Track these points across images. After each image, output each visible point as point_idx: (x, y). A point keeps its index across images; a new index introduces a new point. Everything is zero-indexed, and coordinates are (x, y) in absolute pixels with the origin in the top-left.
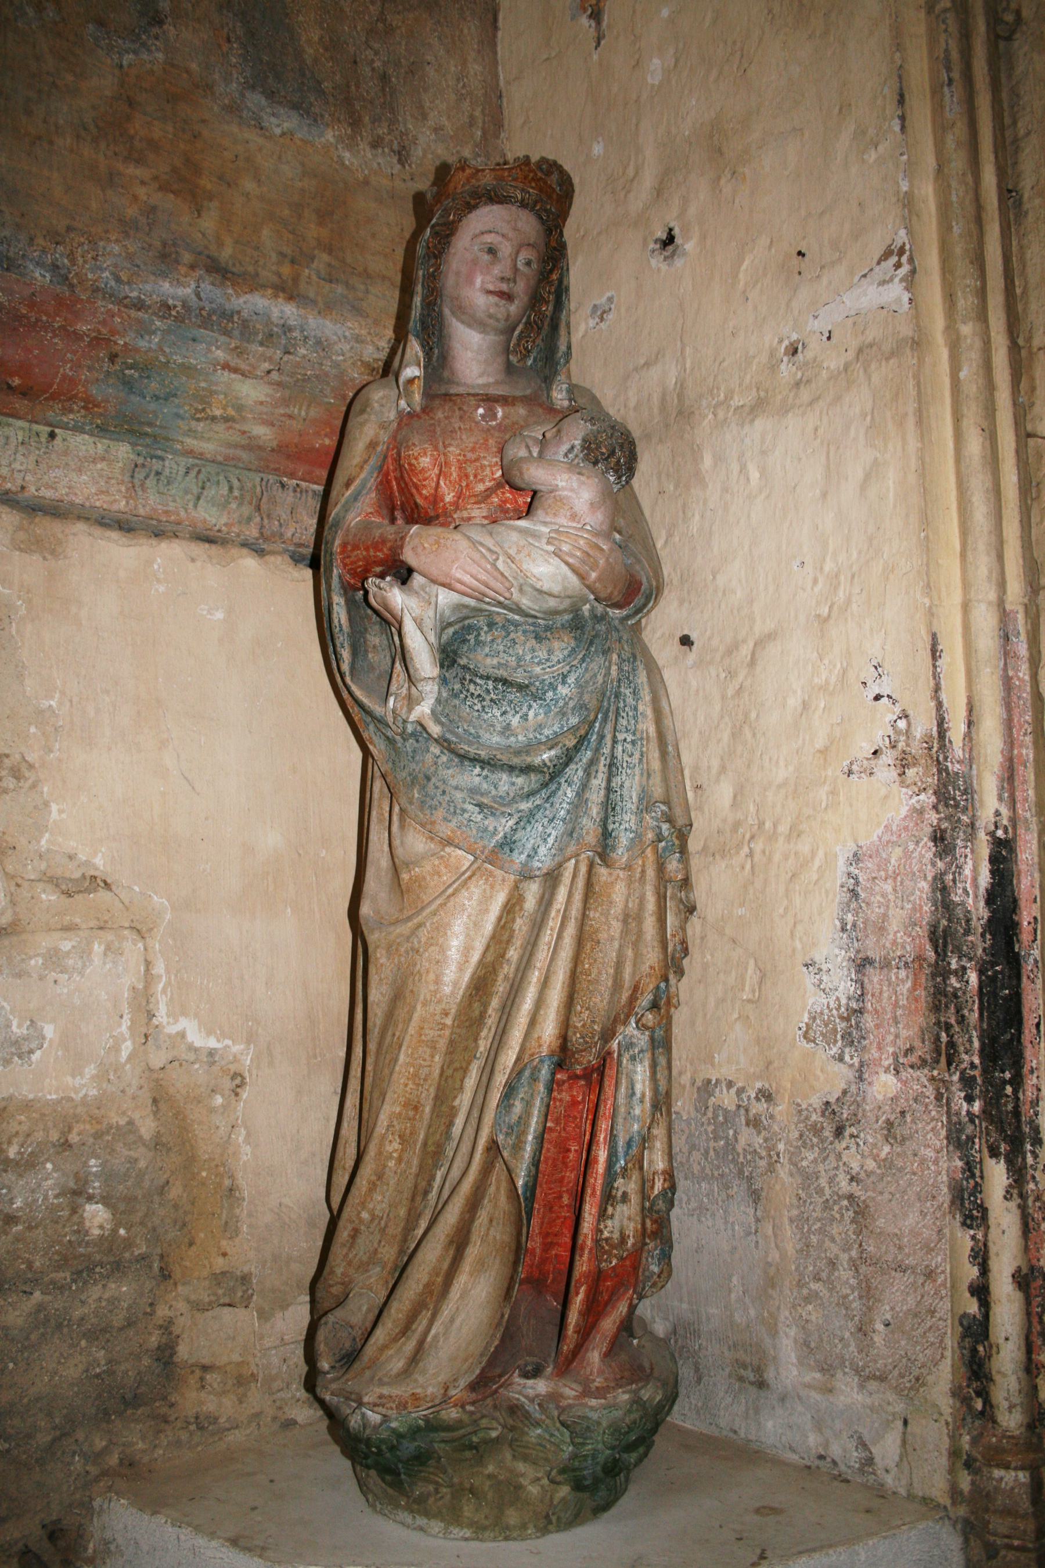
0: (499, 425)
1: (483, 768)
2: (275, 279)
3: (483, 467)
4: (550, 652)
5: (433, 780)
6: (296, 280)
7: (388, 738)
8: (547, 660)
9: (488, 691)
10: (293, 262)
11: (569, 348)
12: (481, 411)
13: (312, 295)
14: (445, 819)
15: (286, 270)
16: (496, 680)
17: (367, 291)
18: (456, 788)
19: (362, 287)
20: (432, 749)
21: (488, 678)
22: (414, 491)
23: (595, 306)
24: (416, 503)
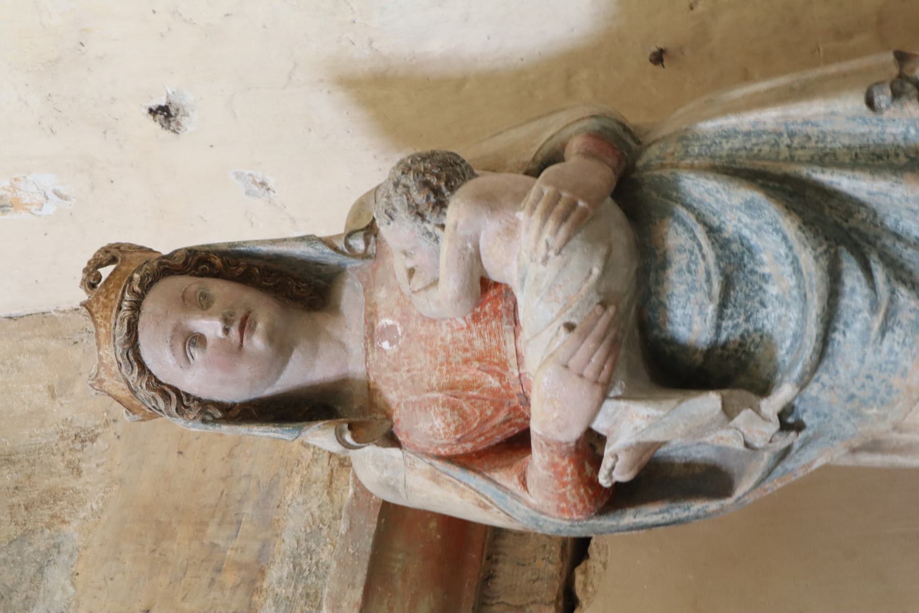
0: (401, 322)
1: (835, 330)
2: (240, 593)
3: (454, 341)
4: (681, 250)
5: (853, 390)
6: (240, 566)
7: (802, 447)
8: (692, 253)
9: (736, 326)
10: (219, 570)
11: (302, 239)
12: (386, 345)
13: (256, 546)
14: (904, 374)
15: (230, 578)
16: (720, 316)
17: (249, 476)
18: (862, 361)
19: (243, 483)
21: (718, 327)
22: (488, 426)
23: (247, 193)
24: (504, 422)
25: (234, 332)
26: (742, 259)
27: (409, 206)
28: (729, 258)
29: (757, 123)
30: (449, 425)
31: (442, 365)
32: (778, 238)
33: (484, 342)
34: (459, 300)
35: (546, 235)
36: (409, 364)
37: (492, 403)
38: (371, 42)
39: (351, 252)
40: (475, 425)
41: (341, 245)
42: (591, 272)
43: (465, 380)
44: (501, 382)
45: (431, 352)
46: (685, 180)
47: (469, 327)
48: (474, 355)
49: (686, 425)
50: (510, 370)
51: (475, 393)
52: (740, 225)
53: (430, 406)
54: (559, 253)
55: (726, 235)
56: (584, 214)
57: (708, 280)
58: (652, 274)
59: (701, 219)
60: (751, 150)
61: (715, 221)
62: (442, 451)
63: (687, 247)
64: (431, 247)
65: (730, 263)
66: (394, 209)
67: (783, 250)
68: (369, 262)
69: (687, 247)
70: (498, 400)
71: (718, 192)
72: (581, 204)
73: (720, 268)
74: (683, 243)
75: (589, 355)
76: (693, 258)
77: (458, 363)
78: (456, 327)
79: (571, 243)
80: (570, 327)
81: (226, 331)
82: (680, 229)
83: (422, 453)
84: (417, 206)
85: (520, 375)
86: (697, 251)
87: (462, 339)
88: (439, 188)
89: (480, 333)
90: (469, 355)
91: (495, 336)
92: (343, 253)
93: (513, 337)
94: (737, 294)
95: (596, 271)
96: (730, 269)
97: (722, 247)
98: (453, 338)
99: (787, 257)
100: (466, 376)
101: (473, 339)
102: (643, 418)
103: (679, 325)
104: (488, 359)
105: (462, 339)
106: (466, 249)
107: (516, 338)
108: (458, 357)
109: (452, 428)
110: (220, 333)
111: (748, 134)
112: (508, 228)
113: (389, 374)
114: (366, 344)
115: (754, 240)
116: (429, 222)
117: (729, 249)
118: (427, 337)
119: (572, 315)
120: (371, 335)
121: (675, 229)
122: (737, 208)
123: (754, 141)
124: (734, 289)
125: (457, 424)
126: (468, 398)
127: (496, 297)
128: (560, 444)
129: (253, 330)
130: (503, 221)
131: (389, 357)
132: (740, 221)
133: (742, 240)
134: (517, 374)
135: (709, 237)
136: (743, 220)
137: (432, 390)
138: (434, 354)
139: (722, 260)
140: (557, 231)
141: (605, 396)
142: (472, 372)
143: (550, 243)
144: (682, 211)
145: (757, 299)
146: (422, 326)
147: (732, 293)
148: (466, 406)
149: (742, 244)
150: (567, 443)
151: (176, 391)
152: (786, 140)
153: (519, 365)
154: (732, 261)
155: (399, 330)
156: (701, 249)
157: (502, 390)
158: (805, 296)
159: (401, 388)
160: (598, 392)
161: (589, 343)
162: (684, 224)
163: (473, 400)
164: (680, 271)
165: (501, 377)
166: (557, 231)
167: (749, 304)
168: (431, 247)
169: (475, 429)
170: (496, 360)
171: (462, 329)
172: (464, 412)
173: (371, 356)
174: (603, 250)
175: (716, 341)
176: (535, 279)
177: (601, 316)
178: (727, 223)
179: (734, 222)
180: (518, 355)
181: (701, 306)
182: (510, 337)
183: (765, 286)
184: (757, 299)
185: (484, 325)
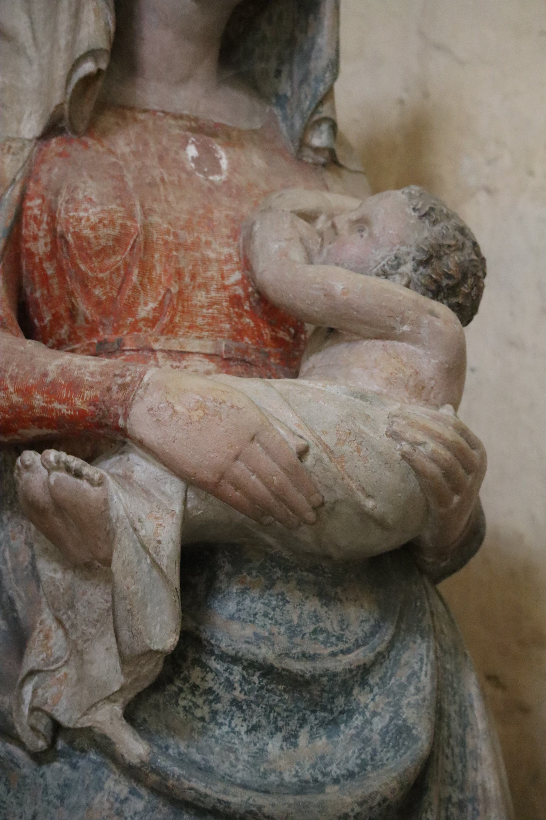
0: (227, 183)
3: (206, 261)
4: (343, 623)
8: (339, 638)
9: (230, 685)
16: (252, 665)
20: (109, 784)
21: (235, 660)
26: (324, 709)
27: (441, 246)
28: (329, 692)
29: (477, 757)
30: (93, 228)
31: (176, 235)
32: (351, 766)
33: (202, 307)
34: (328, 295)
35: (432, 445)
36: (172, 183)
37: (113, 300)
38: (489, 191)
39: (312, 124)
40: (83, 267)
41: (325, 111)
42: (369, 496)
43: (153, 267)
44: (144, 319)
45: (189, 221)
46: (425, 645)
47: (225, 288)
48: (187, 286)
49: (136, 594)
50: (162, 339)
51: (134, 278)
52: (368, 714)
53: (123, 206)
54: (404, 456)
55: (355, 691)
56: (443, 501)
57: (305, 656)
58: (312, 577)
59: (380, 658)
60: (448, 744)
61: (374, 679)
62: (34, 205)
63: (347, 633)
64: (372, 264)
65: (323, 690)
66: (435, 223)
67: (334, 770)
68: (292, 149)
69: (347, 633)
70: (115, 310)
71: (418, 690)
72: (456, 499)
73: (321, 676)
74: (352, 628)
75: (261, 473)
76: (333, 639)
77: (177, 261)
78: (225, 268)
79: (412, 477)
80: (303, 453)
82: (367, 627)
83: (30, 171)
84: (439, 258)
85: (153, 351)
86: (342, 646)
87: (209, 274)
88: (456, 295)
89: (215, 304)
90: (187, 279)
91: (209, 324)
92: (315, 111)
93: (208, 351)
94: (279, 697)
95: (370, 504)
96: (315, 690)
97: (344, 682)
98: (209, 260)
99: (325, 775)
100: (159, 269)
101: (208, 292)
102: (156, 533)
103: (238, 603)
104: (180, 308)
105: (209, 274)
106: (403, 323)
107: (206, 355)
108: (185, 263)
109: (87, 232)
111: (463, 744)
112: (423, 388)
113: (153, 148)
114: (189, 118)
115: (347, 731)
116: (415, 270)
117: (339, 693)
118: (211, 220)
119: (319, 460)
120: (205, 131)
121: (367, 620)
122: (396, 715)
123: (457, 750)
124: (285, 690)
125: (93, 240)
126: (127, 266)
127: (260, 336)
128: (127, 405)
130: (433, 382)
131: (177, 153)
132: (375, 714)
133: (349, 713)
134: (156, 346)
135: (358, 667)
136: (376, 719)
137: (146, 214)
138: (188, 226)
139: (328, 681)
140: (434, 460)
141: (190, 481)
142: (163, 279)
143: (421, 448)
144: (387, 634)
145: (264, 722)
146: (227, 216)
147: (281, 687)
148: (117, 259)
149: (341, 713)
150: (126, 415)
152: (456, 796)
153: (169, 352)
154: (325, 695)
155: (216, 178)
156: (344, 652)
157: (130, 320)
158: (267, 792)
159: (138, 163)
160: (209, 476)
161: (279, 478)
162: (373, 634)
163: (122, 272)
164: (317, 618)
165: (152, 322)
166: (434, 460)
167: (259, 710)
168: (372, 264)
169: (75, 265)
170: (177, 319)
171: (223, 278)
172: (109, 256)
173: (172, 122)
174: (390, 519)
175: (212, 653)
176: (368, 416)
177: (308, 500)
178: (371, 696)
179: (371, 705)
180: (183, 354)
181: (270, 640)
182: (208, 347)
183: (279, 736)
184: (264, 722)
185: (226, 311)
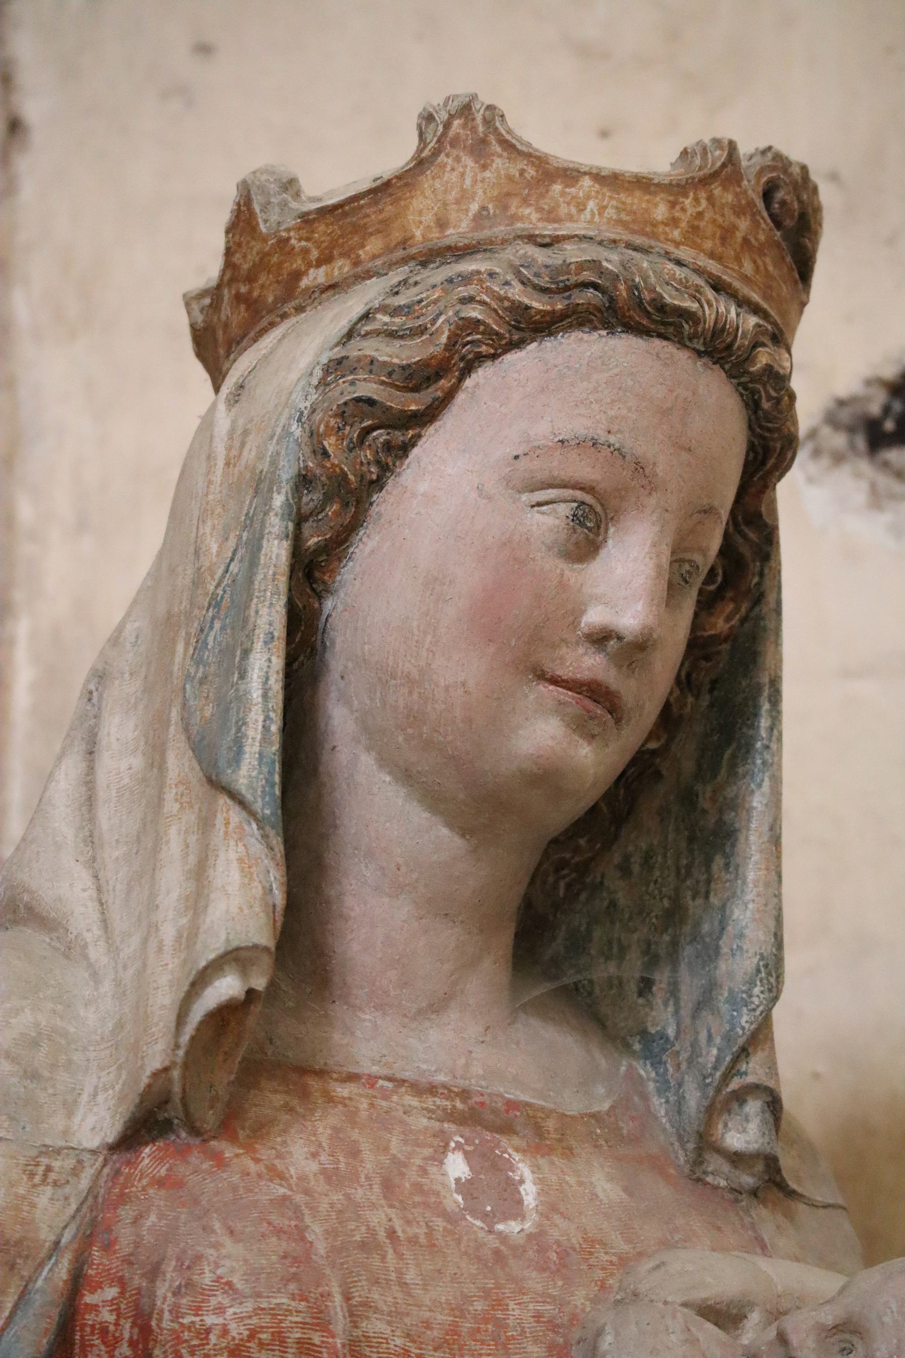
0: (536, 1238)
25: (590, 664)
39: (725, 1102)
41: (754, 1070)
45: (454, 1330)
62: (101, 1299)
81: (601, 638)
92: (731, 1072)
110: (595, 617)
114: (448, 1091)
118: (500, 1325)
120: (482, 1118)
129: (581, 726)
146: (538, 1316)
151: (429, 415)
155: (512, 1227)
173: (412, 1101)
